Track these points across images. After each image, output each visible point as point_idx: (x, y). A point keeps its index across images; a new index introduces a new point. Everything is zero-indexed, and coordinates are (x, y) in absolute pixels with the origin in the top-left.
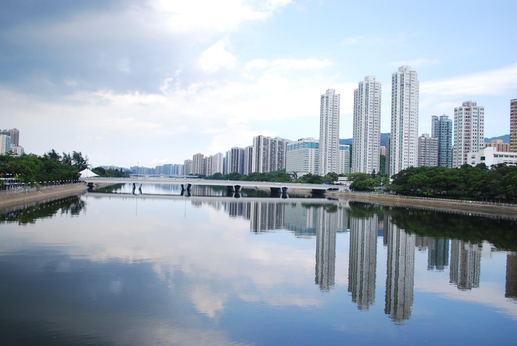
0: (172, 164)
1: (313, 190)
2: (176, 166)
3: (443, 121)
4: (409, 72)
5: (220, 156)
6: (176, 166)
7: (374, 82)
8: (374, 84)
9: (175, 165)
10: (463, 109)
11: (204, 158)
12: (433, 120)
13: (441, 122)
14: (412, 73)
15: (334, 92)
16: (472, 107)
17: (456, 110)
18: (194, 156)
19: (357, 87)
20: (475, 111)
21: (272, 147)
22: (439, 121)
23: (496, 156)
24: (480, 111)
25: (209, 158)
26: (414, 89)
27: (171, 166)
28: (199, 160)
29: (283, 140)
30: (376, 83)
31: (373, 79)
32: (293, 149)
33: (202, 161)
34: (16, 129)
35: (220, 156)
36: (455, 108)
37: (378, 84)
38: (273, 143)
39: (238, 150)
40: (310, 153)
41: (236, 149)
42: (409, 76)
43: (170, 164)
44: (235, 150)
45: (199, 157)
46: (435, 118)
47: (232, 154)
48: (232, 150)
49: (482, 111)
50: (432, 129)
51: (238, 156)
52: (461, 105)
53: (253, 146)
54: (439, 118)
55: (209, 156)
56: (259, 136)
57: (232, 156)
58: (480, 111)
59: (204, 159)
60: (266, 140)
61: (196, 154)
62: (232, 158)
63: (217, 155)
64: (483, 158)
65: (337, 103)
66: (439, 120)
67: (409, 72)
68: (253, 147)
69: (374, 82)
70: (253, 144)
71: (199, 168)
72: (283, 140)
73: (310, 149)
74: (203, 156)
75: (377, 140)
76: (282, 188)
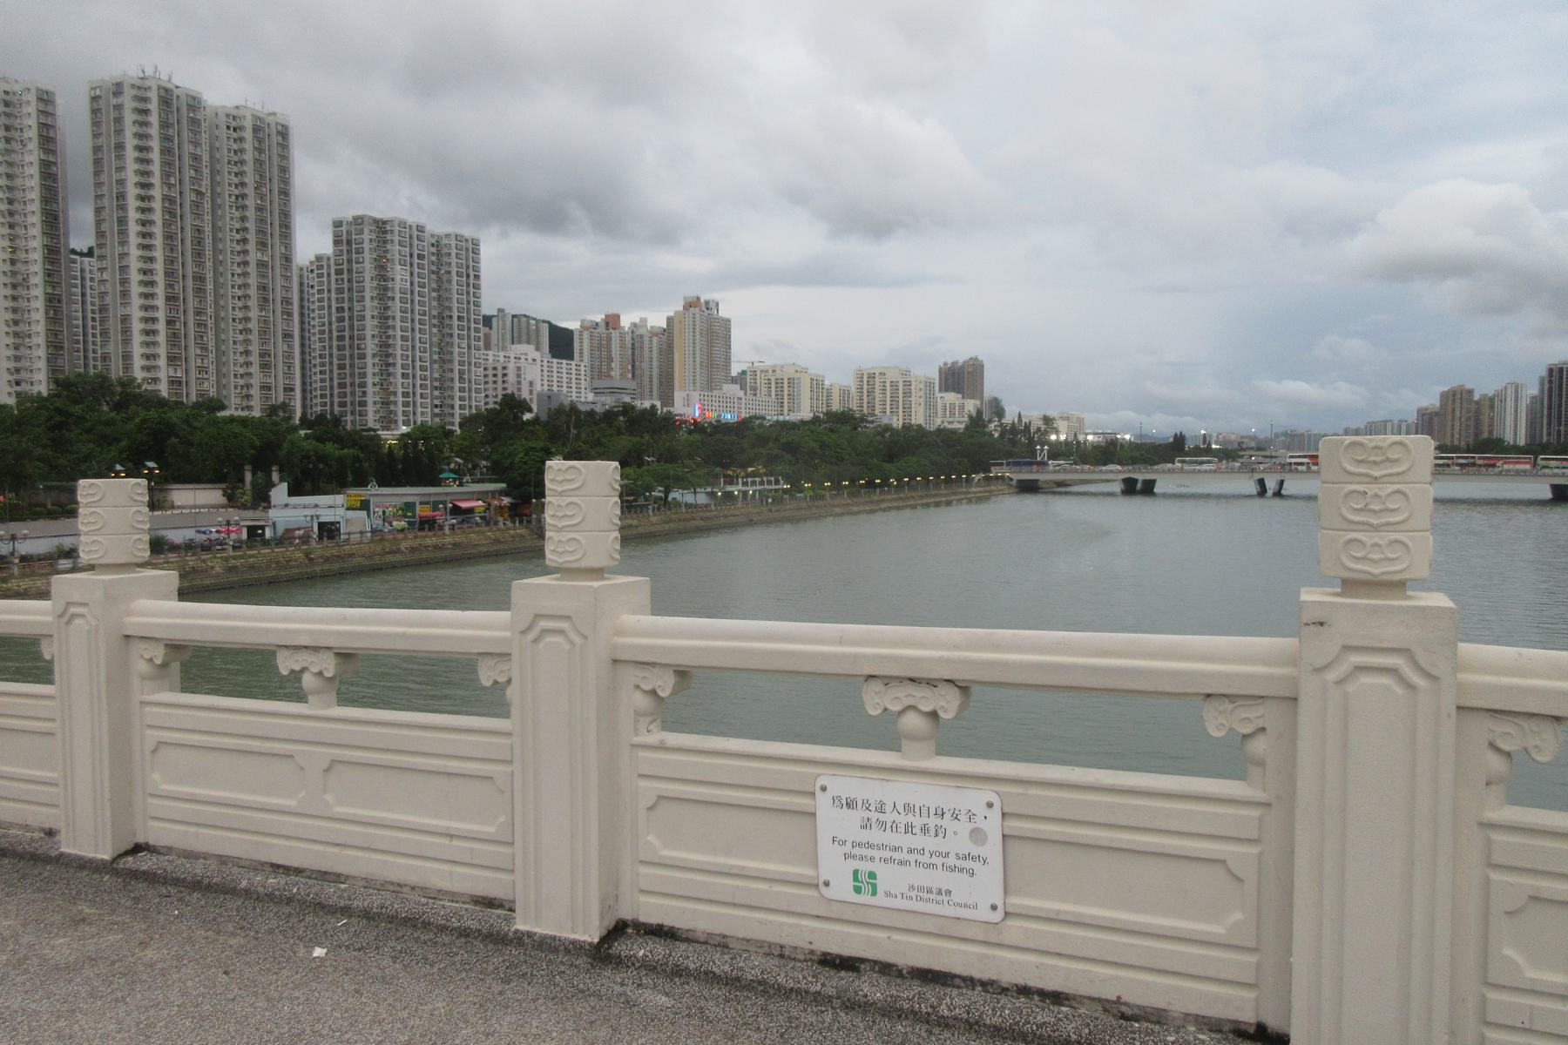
0: (1391, 421)
5: (1517, 392)
9: (1401, 421)
11: (1476, 397)
18: (1445, 396)
25: (1492, 400)
28: (1458, 404)
33: (1469, 411)
34: (976, 359)
35: (1517, 392)
47: (1550, 382)
48: (1551, 371)
55: (1491, 394)
57: (1550, 390)
59: (1477, 403)
63: (1506, 388)
74: (1470, 392)
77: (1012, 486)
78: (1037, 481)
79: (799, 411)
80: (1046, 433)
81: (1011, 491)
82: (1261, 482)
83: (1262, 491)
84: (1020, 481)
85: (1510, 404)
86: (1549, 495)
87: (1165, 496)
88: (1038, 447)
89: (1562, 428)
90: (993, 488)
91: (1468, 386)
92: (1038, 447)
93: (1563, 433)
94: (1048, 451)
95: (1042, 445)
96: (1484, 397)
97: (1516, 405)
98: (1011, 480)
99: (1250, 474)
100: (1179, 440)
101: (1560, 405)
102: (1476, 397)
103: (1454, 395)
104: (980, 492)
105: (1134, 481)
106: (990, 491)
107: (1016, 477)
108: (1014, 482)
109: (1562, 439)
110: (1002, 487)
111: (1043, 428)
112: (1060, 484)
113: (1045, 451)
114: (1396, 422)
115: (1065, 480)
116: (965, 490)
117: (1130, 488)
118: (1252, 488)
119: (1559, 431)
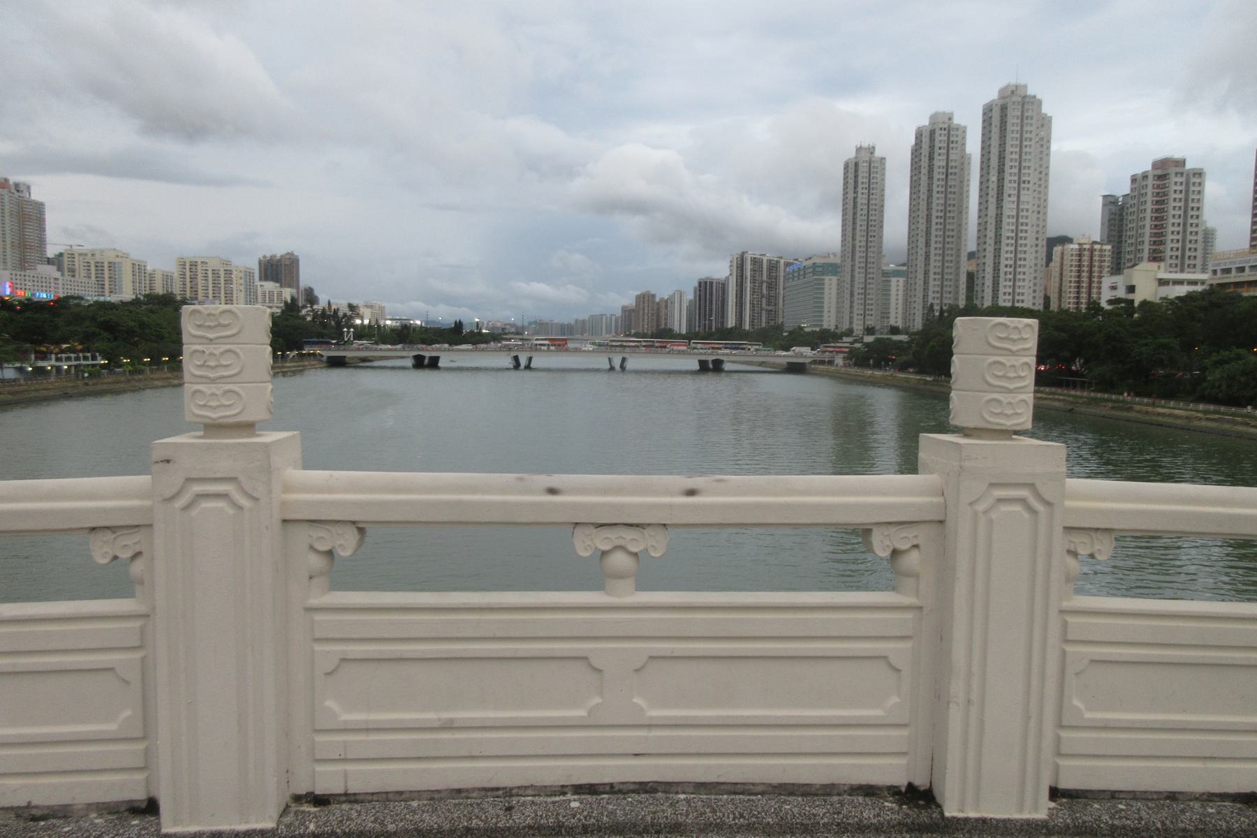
0: (605, 315)
1: (788, 363)
2: (614, 318)
4: (1020, 99)
5: (681, 297)
6: (614, 318)
7: (949, 126)
8: (949, 131)
9: (611, 315)
10: (1150, 178)
11: (657, 300)
12: (1104, 205)
14: (1027, 100)
15: (872, 153)
16: (1173, 170)
19: (912, 141)
20: (1179, 179)
21: (769, 276)
22: (1118, 208)
23: (1163, 282)
24: (1193, 180)
25: (666, 301)
26: (1033, 136)
27: (604, 317)
28: (646, 305)
29: (797, 260)
31: (946, 121)
32: (796, 279)
35: (681, 297)
36: (1132, 176)
37: (957, 129)
38: (773, 267)
39: (712, 282)
40: (826, 287)
42: (1020, 107)
43: (602, 315)
44: (706, 282)
47: (700, 291)
48: (700, 283)
49: (1197, 180)
50: (1103, 224)
51: (711, 294)
52: (1149, 168)
53: (731, 274)
54: (1121, 199)
56: (743, 253)
57: (700, 295)
58: (1193, 180)
59: (658, 304)
61: (641, 294)
62: (700, 300)
64: (1131, 289)
65: (878, 176)
66: (1120, 203)
67: (1020, 99)
68: (730, 277)
69: (949, 126)
70: (731, 270)
71: (646, 321)
72: (797, 260)
73: (827, 278)
74: (654, 296)
76: (713, 361)
77: (323, 361)
78: (345, 357)
79: (121, 292)
80: (351, 318)
81: (322, 366)
82: (516, 358)
83: (517, 366)
84: (329, 358)
85: (677, 305)
86: (697, 367)
88: (345, 330)
89: (707, 322)
90: (306, 363)
91: (652, 292)
92: (345, 330)
93: (707, 325)
94: (354, 332)
95: (349, 328)
96: (662, 300)
97: (681, 305)
98: (322, 356)
99: (508, 352)
100: (459, 326)
101: (705, 306)
102: (657, 300)
103: (644, 298)
104: (294, 367)
106: (303, 366)
107: (326, 354)
108: (325, 359)
109: (707, 330)
110: (313, 363)
111: (349, 313)
112: (364, 360)
113: (351, 333)
114: (609, 316)
115: (368, 357)
116: (280, 365)
117: (419, 363)
118: (507, 361)
119: (705, 324)
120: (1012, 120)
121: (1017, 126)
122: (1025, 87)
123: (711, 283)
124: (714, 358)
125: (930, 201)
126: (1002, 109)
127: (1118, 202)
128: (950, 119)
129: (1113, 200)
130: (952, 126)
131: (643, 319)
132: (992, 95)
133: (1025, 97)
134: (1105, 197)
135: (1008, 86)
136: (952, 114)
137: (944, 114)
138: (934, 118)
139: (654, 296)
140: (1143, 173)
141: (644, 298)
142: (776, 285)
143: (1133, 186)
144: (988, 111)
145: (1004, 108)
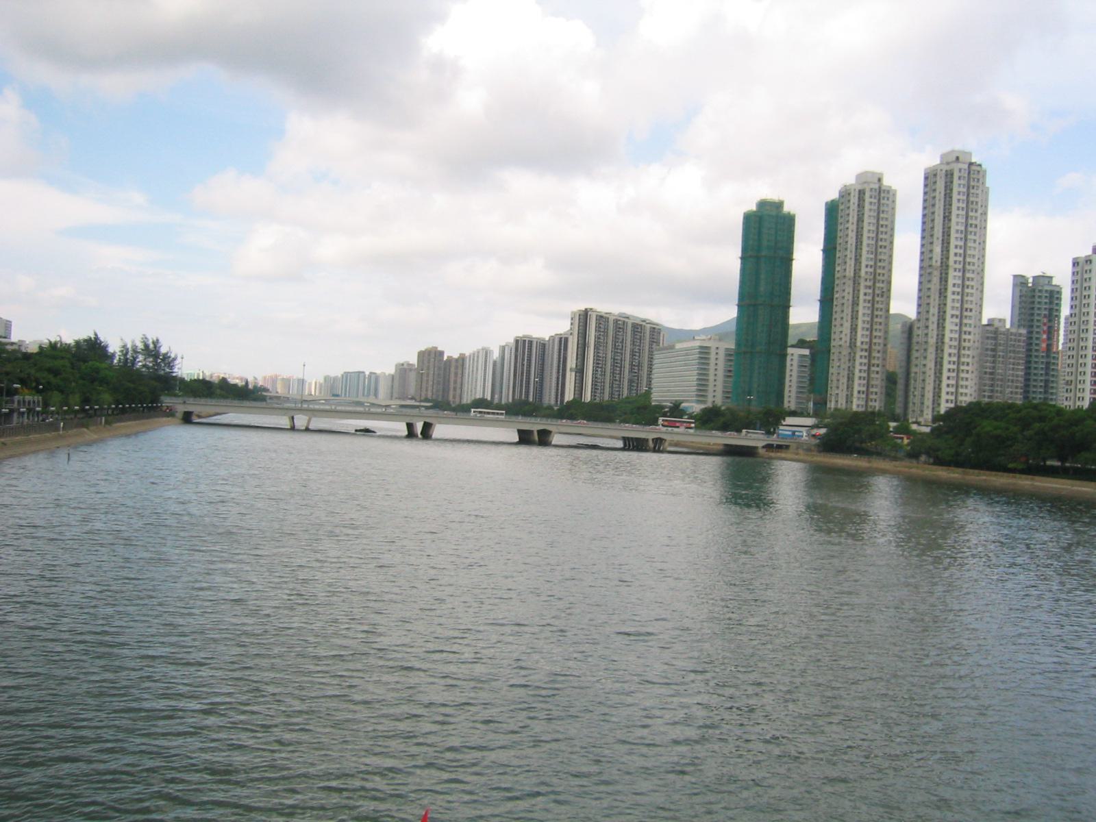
0: (363, 372)
2: (373, 376)
3: (1040, 288)
5: (486, 356)
6: (373, 376)
7: (880, 188)
9: (371, 373)
11: (445, 358)
12: (1015, 285)
13: (1034, 291)
17: (1076, 263)
18: (423, 355)
25: (457, 360)
27: (361, 375)
28: (431, 364)
30: (884, 191)
31: (876, 181)
33: (439, 368)
35: (486, 356)
36: (1074, 259)
37: (888, 192)
41: (527, 339)
43: (359, 372)
44: (524, 341)
45: (433, 355)
46: (1019, 281)
48: (517, 341)
50: (1013, 306)
53: (571, 334)
54: (1031, 280)
55: (456, 356)
56: (586, 309)
60: (602, 319)
61: (426, 350)
63: (478, 352)
67: (966, 166)
69: (880, 188)
71: (431, 383)
74: (442, 353)
75: (880, 330)
76: (653, 439)
82: (410, 426)
83: (411, 434)
86: (517, 439)
87: (556, 446)
91: (439, 349)
96: (450, 359)
102: (445, 358)
103: (429, 355)
105: (530, 432)
114: (367, 373)
117: (525, 438)
118: (402, 429)
120: (958, 187)
121: (964, 195)
122: (970, 154)
123: (531, 342)
124: (655, 436)
125: (857, 267)
126: (946, 175)
127: (1028, 283)
128: (880, 180)
129: (1023, 281)
130: (883, 188)
131: (427, 381)
132: (931, 159)
133: (971, 164)
134: (1015, 276)
135: (953, 151)
136: (882, 174)
137: (873, 173)
138: (862, 177)
139: (442, 353)
140: (1086, 257)
141: (429, 355)
142: (622, 349)
143: (1075, 270)
144: (930, 178)
145: (949, 175)
